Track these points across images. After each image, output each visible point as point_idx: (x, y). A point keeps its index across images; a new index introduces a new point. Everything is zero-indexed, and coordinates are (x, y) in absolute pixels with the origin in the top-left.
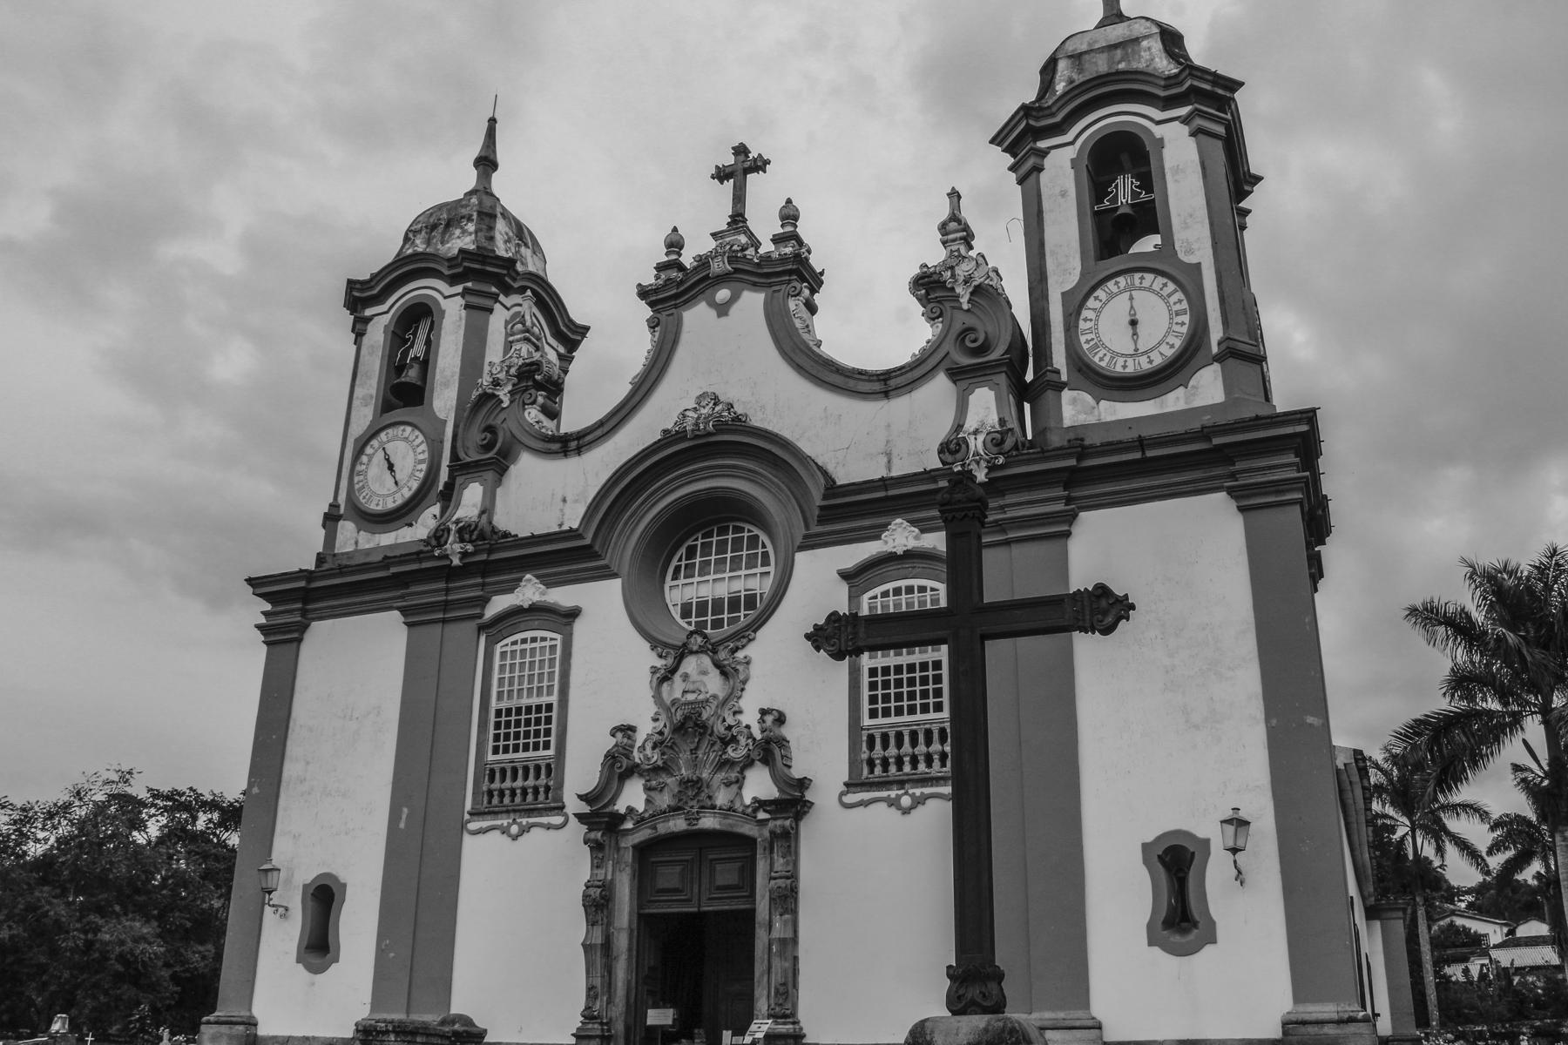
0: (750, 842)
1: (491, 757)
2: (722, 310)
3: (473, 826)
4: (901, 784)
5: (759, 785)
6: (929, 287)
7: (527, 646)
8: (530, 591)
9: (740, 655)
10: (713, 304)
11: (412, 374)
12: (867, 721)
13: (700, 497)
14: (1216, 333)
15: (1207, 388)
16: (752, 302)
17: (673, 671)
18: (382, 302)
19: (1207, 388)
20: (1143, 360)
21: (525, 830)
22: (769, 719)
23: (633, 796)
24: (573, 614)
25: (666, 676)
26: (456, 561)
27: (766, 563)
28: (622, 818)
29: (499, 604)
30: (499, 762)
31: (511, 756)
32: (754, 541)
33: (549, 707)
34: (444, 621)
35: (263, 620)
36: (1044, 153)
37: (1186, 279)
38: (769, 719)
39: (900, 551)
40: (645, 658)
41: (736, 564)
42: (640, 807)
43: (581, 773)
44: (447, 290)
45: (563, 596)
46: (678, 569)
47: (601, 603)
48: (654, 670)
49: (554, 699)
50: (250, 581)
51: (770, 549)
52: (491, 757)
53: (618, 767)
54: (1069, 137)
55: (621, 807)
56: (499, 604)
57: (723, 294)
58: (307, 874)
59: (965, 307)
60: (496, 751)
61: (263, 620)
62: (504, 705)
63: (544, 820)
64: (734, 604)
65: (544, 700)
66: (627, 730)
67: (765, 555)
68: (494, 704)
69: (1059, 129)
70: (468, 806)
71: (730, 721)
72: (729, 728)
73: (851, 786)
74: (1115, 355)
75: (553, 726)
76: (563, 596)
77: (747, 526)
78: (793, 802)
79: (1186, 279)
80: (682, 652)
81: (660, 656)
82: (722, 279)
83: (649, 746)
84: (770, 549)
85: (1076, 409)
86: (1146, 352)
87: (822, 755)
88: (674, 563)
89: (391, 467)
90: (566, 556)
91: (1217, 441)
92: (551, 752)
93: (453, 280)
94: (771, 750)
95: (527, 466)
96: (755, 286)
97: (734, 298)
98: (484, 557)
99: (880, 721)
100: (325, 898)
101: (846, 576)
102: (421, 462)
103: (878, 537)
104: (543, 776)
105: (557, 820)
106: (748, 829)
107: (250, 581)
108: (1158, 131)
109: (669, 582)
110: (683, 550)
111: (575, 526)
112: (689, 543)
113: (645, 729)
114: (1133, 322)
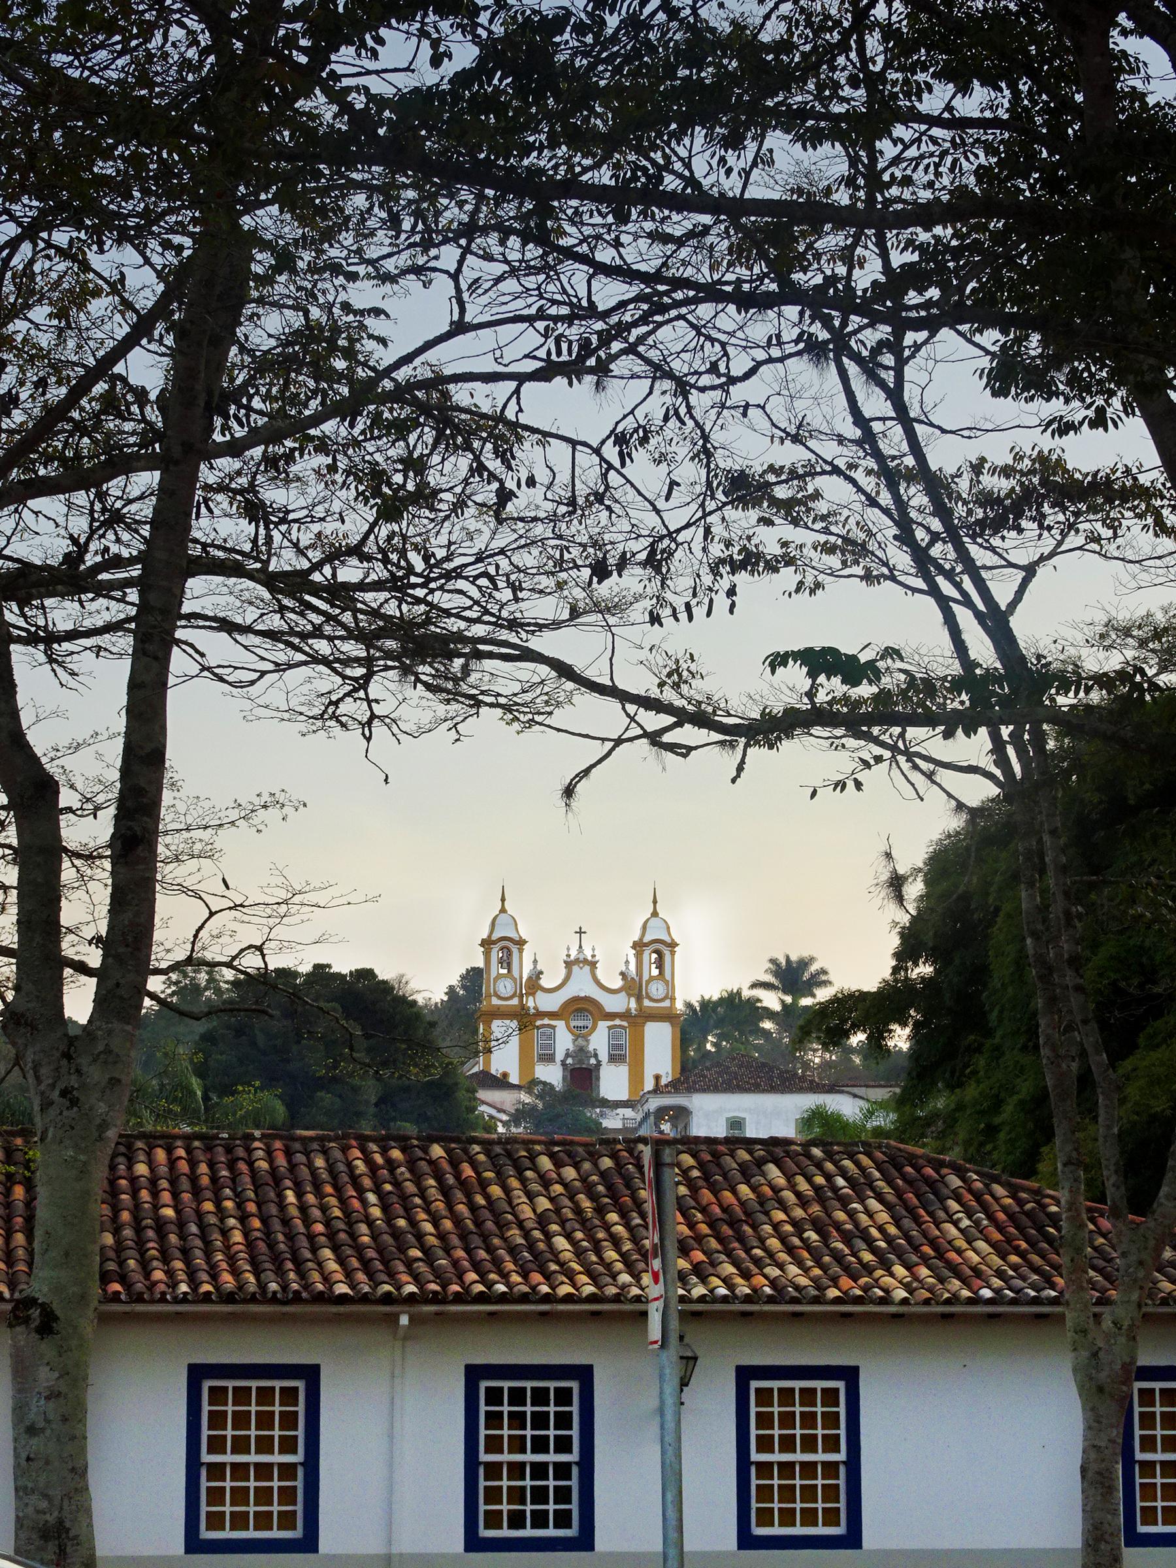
5: (593, 1061)
6: (622, 974)
8: (546, 1021)
13: (581, 1009)
15: (667, 1004)
16: (587, 968)
19: (667, 1004)
23: (569, 1061)
29: (538, 1023)
37: (667, 983)
40: (570, 1037)
43: (559, 1056)
45: (553, 1023)
47: (560, 1025)
53: (567, 1055)
56: (538, 1023)
76: (553, 1023)
79: (667, 983)
85: (647, 1003)
87: (604, 1056)
90: (552, 1015)
94: (596, 1056)
95: (539, 994)
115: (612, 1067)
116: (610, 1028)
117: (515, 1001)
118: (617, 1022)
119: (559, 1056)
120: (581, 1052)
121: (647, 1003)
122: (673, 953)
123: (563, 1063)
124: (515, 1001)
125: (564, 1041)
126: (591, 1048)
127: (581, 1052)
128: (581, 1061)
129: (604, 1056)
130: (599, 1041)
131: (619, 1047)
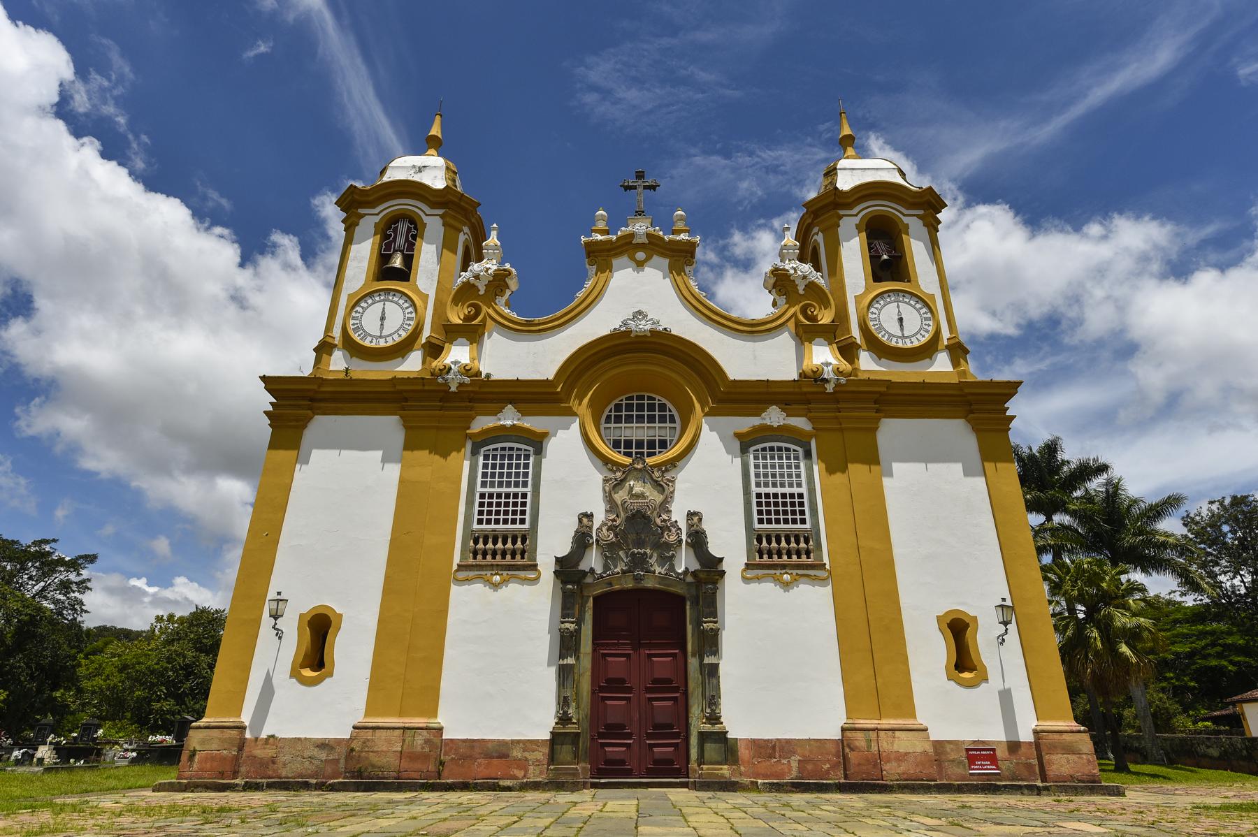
0: (681, 600)
1: (476, 526)
2: (640, 265)
3: (462, 575)
4: (783, 567)
5: (684, 561)
7: (507, 453)
8: (509, 418)
9: (668, 476)
10: (633, 258)
11: (397, 262)
12: (757, 526)
14: (946, 334)
17: (623, 481)
18: (374, 207)
20: (908, 341)
21: (504, 582)
22: (696, 519)
24: (545, 435)
25: (619, 484)
26: (453, 389)
27: (672, 420)
28: (584, 574)
29: (482, 423)
30: (482, 531)
31: (493, 526)
32: (663, 407)
33: (524, 496)
34: (438, 428)
35: (270, 408)
36: (840, 217)
37: (925, 302)
38: (696, 519)
39: (775, 425)
41: (651, 419)
42: (599, 570)
43: (553, 542)
44: (428, 211)
46: (609, 417)
48: (606, 481)
49: (528, 490)
50: (263, 378)
51: (675, 413)
52: (476, 526)
53: (582, 540)
54: (855, 211)
55: (584, 566)
56: (482, 423)
57: (640, 255)
58: (300, 605)
59: (801, 292)
60: (480, 522)
61: (270, 408)
62: (488, 490)
63: (522, 574)
64: (651, 444)
65: (520, 490)
66: (590, 516)
67: (672, 417)
68: (479, 489)
69: (849, 206)
70: (457, 560)
71: (664, 517)
72: (664, 521)
73: (748, 566)
74: (891, 335)
75: (528, 509)
77: (657, 397)
78: (711, 569)
79: (925, 302)
80: (628, 471)
81: (611, 470)
82: (641, 247)
83: (604, 529)
84: (675, 413)
85: (867, 363)
86: (909, 337)
87: (729, 541)
88: (606, 413)
89: (383, 319)
91: (967, 391)
92: (526, 526)
93: (433, 205)
94: (698, 540)
96: (662, 255)
97: (648, 258)
98: (477, 389)
99: (765, 526)
100: (320, 628)
101: (737, 435)
102: (409, 319)
103: (759, 415)
104: (519, 542)
105: (532, 575)
106: (678, 590)
107: (263, 378)
108: (906, 220)
109: (603, 425)
110: (612, 406)
111: (551, 378)
112: (617, 401)
113: (600, 517)
114: (899, 321)
115: (767, 590)
116: (746, 442)
117: (413, 364)
118: (774, 417)
119: (553, 542)
120: (639, 529)
121: (867, 363)
122: (932, 226)
123: (567, 569)
124: (413, 364)
125: (571, 483)
126: (678, 514)
127: (639, 529)
128: (639, 562)
129: (729, 541)
130: (710, 485)
131: (792, 507)
